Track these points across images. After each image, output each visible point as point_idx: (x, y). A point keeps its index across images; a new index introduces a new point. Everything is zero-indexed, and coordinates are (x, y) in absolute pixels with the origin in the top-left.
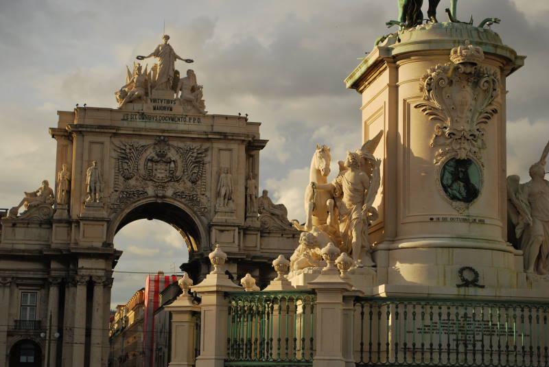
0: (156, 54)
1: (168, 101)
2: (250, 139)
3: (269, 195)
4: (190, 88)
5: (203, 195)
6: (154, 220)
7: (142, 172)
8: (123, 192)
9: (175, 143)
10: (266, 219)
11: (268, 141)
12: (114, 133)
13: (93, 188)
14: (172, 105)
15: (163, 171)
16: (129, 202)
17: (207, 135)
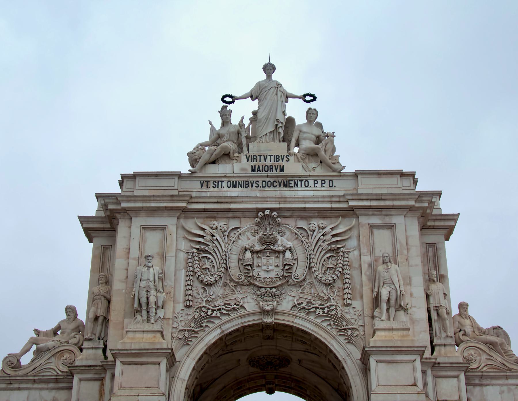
0: (253, 96)
1: (277, 158)
2: (426, 205)
3: (471, 312)
4: (314, 138)
5: (349, 305)
6: (277, 393)
7: (235, 272)
8: (201, 307)
9: (291, 223)
10: (472, 352)
11: (458, 215)
12: (184, 211)
13: (144, 300)
14: (284, 163)
15: (271, 268)
16: (210, 325)
17: (347, 202)
